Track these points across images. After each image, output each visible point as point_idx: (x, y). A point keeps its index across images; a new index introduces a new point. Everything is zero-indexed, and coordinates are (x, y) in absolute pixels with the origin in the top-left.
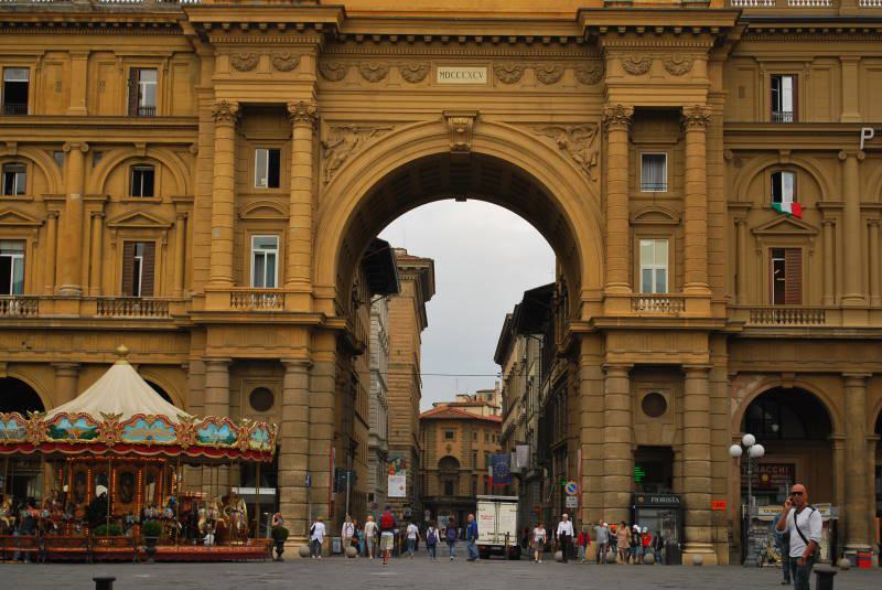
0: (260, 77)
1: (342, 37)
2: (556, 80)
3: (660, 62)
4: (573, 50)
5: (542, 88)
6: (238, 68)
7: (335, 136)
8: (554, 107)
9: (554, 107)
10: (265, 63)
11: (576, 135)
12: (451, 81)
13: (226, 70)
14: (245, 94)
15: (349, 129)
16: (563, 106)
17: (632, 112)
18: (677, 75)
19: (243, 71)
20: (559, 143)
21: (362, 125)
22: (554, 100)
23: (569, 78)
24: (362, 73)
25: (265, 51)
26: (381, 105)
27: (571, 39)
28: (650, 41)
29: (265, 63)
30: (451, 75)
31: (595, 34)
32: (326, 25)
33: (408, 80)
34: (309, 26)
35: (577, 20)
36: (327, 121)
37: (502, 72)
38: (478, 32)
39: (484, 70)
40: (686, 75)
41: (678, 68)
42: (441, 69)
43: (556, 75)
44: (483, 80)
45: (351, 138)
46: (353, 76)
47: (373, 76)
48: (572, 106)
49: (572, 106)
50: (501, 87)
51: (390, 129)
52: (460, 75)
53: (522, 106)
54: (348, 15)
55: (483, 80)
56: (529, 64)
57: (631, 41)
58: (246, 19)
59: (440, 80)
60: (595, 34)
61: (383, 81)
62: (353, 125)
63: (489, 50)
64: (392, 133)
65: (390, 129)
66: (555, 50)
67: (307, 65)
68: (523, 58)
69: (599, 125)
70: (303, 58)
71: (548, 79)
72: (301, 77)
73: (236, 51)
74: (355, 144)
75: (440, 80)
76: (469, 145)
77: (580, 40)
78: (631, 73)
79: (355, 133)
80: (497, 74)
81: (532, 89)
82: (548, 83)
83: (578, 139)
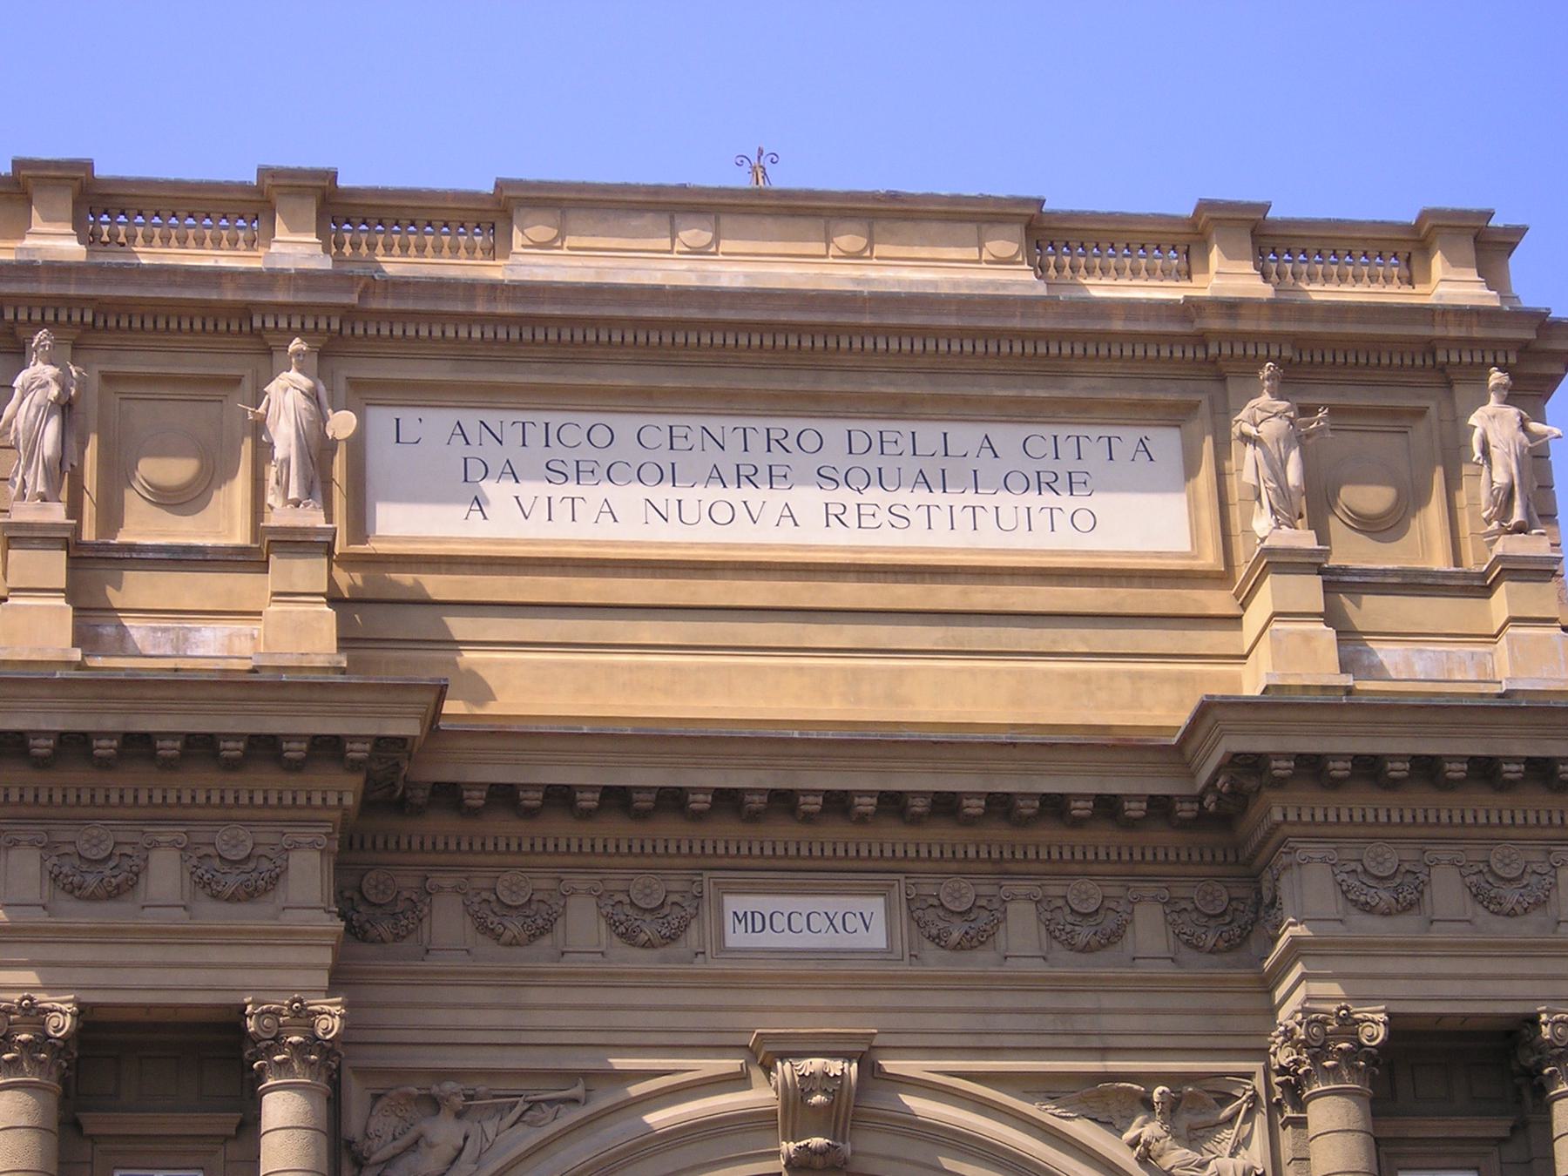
0: (151, 919)
1: (420, 796)
2: (1112, 938)
3: (1453, 873)
4: (1161, 837)
5: (1068, 965)
6: (75, 891)
7: (384, 1124)
8: (1108, 1023)
9: (1108, 1023)
10: (165, 874)
11: (1185, 1119)
12: (768, 940)
13: (33, 895)
14: (100, 976)
15: (435, 1104)
16: (1135, 1023)
17: (1381, 1032)
18: (1512, 914)
19: (93, 898)
20: (1133, 1144)
21: (482, 1087)
22: (1107, 1001)
23: (1149, 930)
24: (475, 916)
25: (166, 834)
26: (541, 1018)
27: (1160, 806)
28: (1422, 802)
29: (165, 874)
30: (768, 921)
31: (1250, 783)
32: (381, 743)
33: (629, 937)
34: (328, 748)
35: (1179, 747)
36: (361, 1072)
37: (930, 915)
38: (863, 780)
39: (875, 907)
40: (1536, 917)
41: (1511, 896)
42: (733, 904)
43: (1110, 922)
44: (877, 938)
45: (444, 1132)
46: (448, 921)
47: (514, 927)
48: (1164, 1023)
49: (1164, 1023)
50: (935, 961)
51: (575, 1101)
52: (799, 922)
53: (1003, 1022)
54: (443, 724)
55: (877, 938)
56: (1021, 887)
57: (1363, 804)
58: (111, 723)
59: (736, 937)
60: (1250, 783)
61: (546, 941)
62: (449, 1086)
63: (895, 836)
64: (578, 1114)
65: (575, 1101)
66: (1103, 837)
67: (308, 875)
68: (1001, 870)
69: (1258, 1082)
70: (295, 858)
71: (1084, 934)
72: (292, 920)
73: (64, 834)
74: (461, 1151)
75: (736, 937)
76: (847, 1148)
77: (1186, 810)
78: (1367, 908)
79: (459, 1115)
80: (923, 921)
81: (1037, 967)
82: (1087, 949)
83: (1191, 1129)
